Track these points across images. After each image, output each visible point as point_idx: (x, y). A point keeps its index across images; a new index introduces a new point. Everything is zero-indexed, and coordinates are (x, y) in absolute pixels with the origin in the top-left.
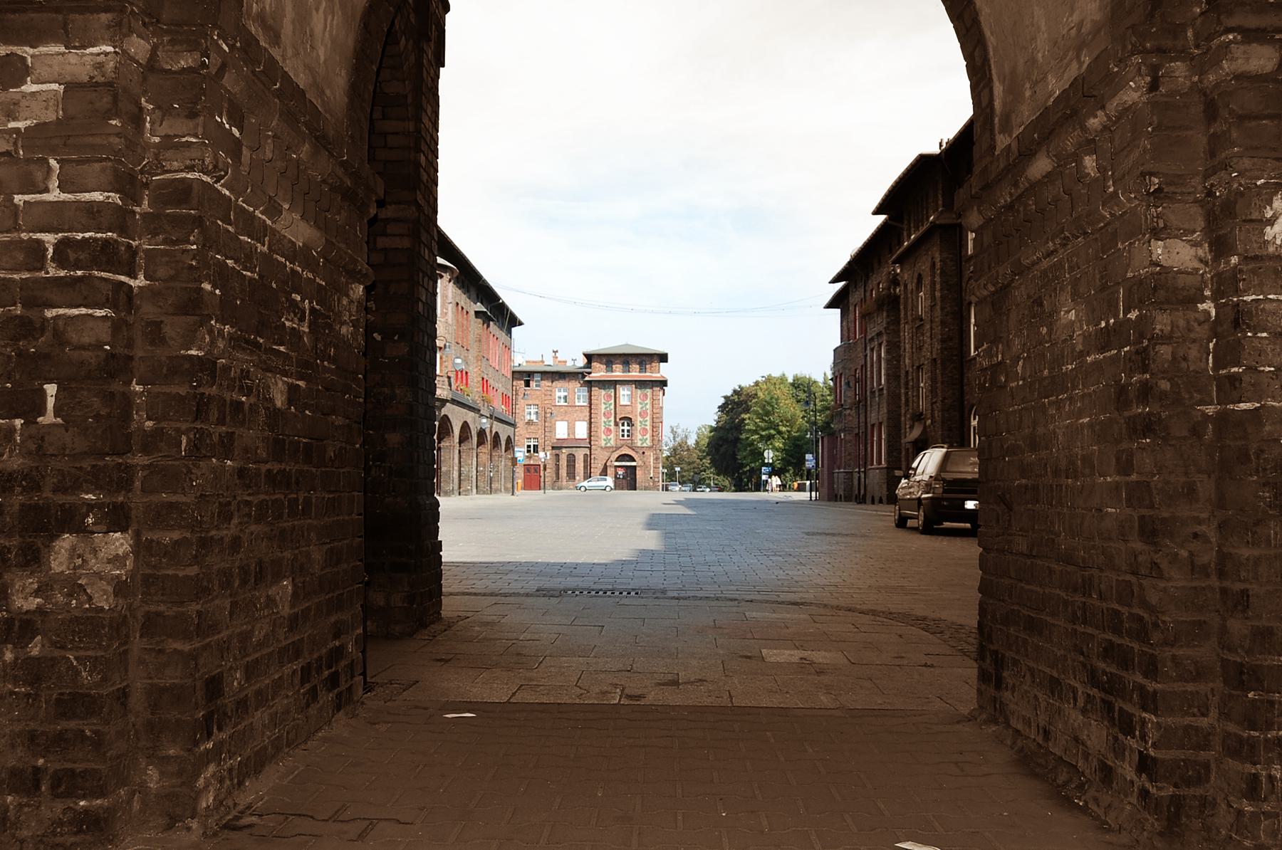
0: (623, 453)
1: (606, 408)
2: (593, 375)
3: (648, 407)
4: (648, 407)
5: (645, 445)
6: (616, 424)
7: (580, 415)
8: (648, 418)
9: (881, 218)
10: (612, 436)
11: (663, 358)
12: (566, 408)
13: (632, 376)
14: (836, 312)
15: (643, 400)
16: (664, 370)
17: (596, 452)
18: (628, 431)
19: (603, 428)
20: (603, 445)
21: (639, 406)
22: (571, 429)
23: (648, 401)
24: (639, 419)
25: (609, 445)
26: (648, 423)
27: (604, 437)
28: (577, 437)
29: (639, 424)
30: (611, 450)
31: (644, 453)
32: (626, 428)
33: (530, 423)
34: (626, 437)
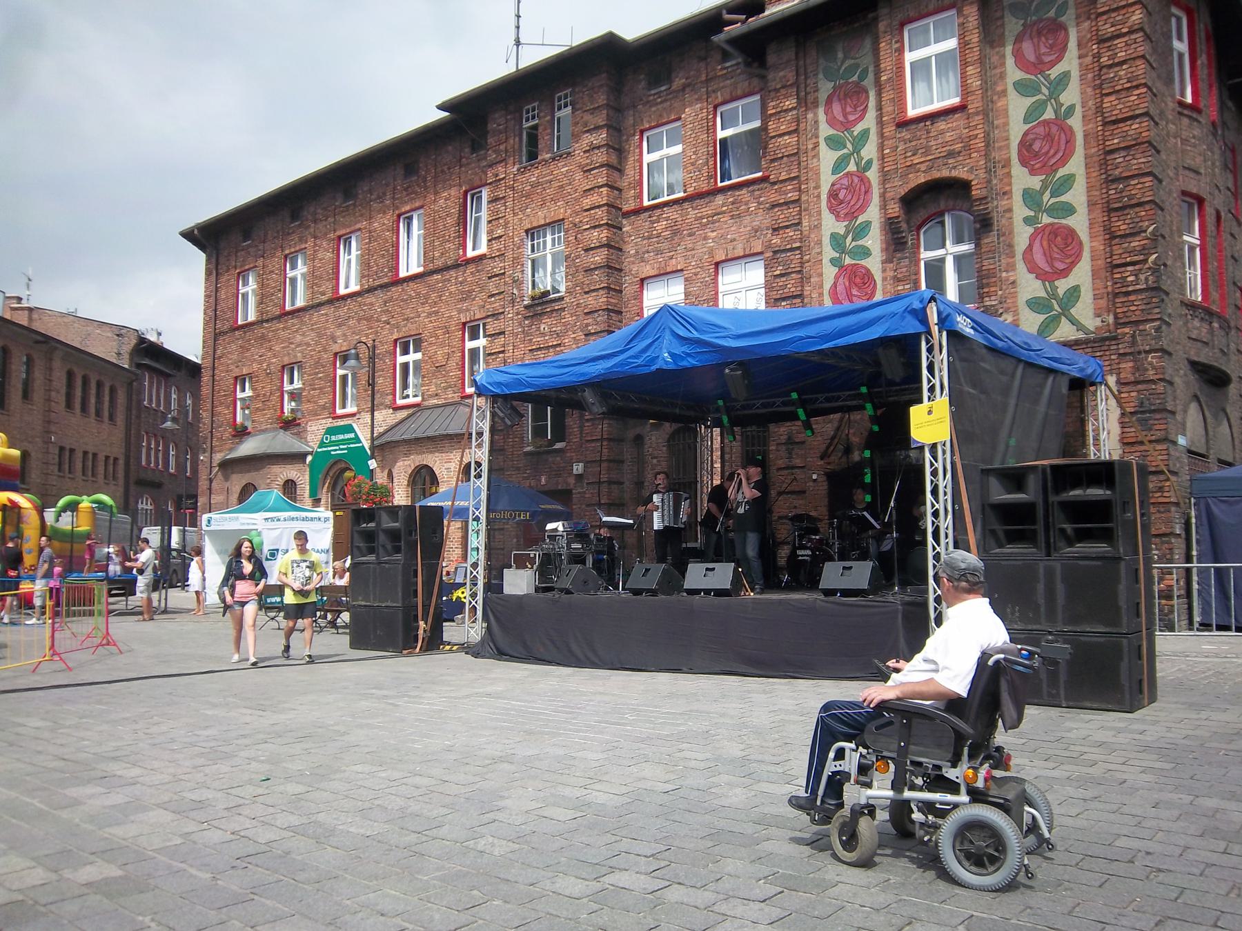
4: (1071, 95)
5: (1066, 331)
8: (1076, 165)
19: (830, 272)
23: (1070, 63)
24: (1022, 179)
26: (1077, 196)
29: (1021, 211)
33: (542, 304)
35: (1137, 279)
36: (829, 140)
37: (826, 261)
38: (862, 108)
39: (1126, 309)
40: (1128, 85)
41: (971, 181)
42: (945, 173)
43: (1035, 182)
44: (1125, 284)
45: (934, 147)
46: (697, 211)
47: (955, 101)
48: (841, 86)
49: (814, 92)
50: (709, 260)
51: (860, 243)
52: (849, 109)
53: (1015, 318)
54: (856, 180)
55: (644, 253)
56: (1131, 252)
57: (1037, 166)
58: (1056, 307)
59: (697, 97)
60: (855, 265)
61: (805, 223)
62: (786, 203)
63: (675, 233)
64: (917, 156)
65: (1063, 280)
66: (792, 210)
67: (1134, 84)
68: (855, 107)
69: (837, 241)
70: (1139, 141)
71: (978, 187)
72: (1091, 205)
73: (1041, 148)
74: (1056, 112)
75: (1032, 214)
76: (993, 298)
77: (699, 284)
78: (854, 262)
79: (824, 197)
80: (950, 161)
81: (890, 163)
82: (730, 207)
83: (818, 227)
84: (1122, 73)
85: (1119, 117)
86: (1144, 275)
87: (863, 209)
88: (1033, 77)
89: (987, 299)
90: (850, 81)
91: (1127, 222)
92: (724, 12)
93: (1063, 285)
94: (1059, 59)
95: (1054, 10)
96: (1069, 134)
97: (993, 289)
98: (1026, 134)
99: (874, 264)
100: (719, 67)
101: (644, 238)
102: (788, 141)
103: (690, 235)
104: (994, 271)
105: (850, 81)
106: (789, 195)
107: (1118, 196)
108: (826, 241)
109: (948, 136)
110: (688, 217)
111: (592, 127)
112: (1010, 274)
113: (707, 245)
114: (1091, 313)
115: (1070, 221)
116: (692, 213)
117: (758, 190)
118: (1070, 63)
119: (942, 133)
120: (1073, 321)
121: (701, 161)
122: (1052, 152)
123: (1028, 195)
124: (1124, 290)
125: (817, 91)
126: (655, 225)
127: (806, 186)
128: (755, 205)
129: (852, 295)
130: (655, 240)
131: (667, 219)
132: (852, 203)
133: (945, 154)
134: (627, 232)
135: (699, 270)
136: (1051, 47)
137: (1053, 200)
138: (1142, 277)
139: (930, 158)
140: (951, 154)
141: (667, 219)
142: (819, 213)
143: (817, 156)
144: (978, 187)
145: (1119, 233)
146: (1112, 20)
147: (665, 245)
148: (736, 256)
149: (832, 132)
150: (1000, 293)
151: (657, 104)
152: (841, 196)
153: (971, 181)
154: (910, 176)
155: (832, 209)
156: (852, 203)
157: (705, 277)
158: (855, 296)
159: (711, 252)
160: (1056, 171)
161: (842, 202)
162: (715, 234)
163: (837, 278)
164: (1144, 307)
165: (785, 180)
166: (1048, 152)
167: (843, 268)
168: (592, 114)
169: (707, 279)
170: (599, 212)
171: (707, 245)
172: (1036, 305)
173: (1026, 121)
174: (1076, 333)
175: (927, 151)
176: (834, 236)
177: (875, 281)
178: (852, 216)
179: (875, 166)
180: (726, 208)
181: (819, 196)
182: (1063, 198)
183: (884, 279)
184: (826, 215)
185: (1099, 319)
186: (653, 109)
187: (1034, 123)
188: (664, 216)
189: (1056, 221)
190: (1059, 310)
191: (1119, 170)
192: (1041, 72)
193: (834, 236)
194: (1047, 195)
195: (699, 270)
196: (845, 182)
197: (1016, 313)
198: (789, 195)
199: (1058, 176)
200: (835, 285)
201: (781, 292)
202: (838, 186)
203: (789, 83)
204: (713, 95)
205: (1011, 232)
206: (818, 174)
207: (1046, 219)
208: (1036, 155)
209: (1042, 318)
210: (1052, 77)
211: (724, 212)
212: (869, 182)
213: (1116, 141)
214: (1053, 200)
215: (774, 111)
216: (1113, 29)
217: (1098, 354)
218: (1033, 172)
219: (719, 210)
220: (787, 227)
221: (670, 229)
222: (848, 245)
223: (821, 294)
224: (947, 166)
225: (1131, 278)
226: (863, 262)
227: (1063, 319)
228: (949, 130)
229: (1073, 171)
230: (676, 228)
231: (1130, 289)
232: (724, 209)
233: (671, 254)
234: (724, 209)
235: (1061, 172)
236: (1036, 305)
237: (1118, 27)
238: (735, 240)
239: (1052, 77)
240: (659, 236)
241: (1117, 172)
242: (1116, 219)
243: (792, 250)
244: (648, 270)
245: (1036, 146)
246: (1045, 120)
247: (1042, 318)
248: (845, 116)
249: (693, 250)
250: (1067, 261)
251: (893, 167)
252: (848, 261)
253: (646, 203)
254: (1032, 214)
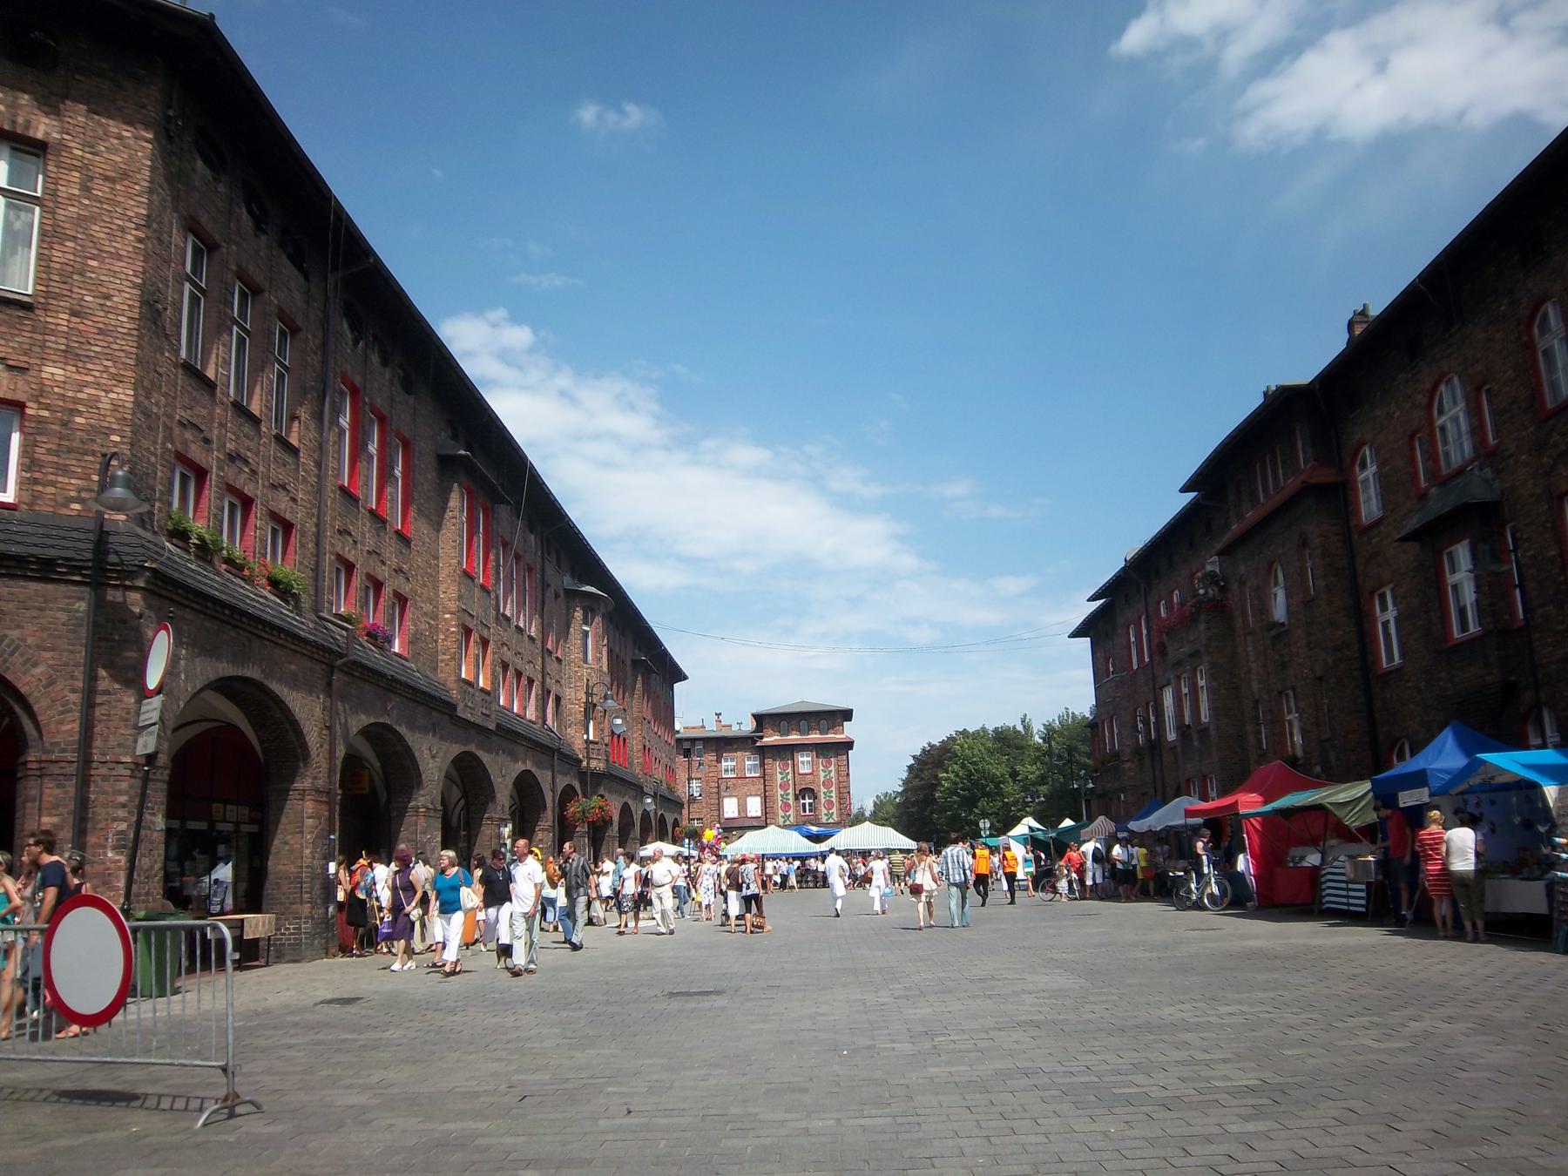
2: (765, 740)
3: (832, 774)
4: (832, 774)
5: (831, 821)
6: (796, 798)
8: (833, 788)
9: (1191, 495)
10: (791, 812)
11: (847, 715)
14: (1085, 642)
15: (826, 767)
16: (849, 730)
18: (810, 804)
19: (780, 803)
21: (822, 774)
22: (742, 807)
23: (832, 768)
24: (823, 790)
26: (833, 794)
27: (781, 813)
28: (749, 815)
29: (823, 796)
32: (807, 801)
34: (807, 813)
47: (810, 771)
99: (791, 802)
118: (832, 768)
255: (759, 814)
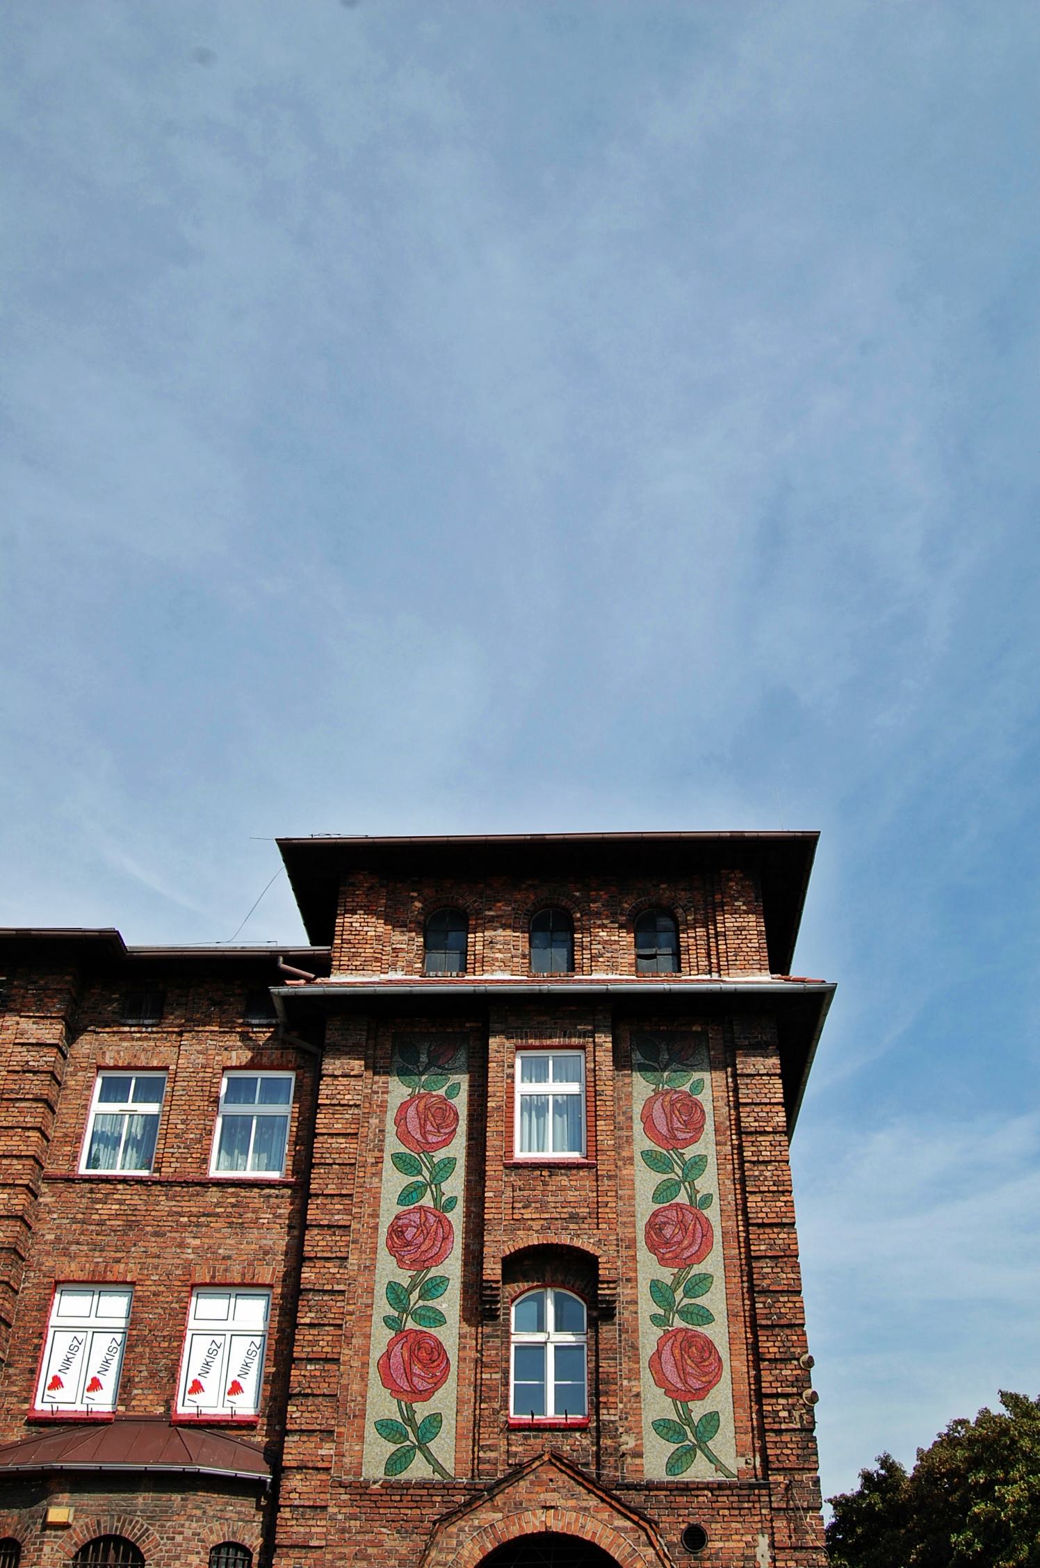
0: (534, 1522)
1: (404, 1198)
4: (708, 1182)
5: (700, 1471)
7: (228, 1244)
8: (714, 1264)
12: (135, 1198)
13: (598, 982)
17: (317, 1530)
19: (381, 1337)
20: (374, 1471)
21: (646, 1181)
23: (706, 1146)
24: (649, 1268)
25: (419, 1469)
26: (716, 1300)
28: (185, 1407)
29: (647, 1307)
30: (432, 1513)
31: (695, 1538)
35: (790, 1416)
36: (397, 1158)
37: (377, 1319)
38: (447, 1131)
39: (779, 1452)
40: (775, 1188)
41: (600, 1257)
42: (565, 1240)
43: (667, 1275)
44: (777, 1419)
45: (553, 1205)
46: (174, 1203)
48: (421, 1097)
49: (383, 1093)
50: (182, 1278)
51: (430, 1303)
52: (429, 1127)
53: (639, 1442)
54: (432, 1219)
55: (70, 1243)
56: (783, 1381)
57: (667, 1256)
58: (690, 1435)
59: (199, 1048)
60: (422, 1332)
61: (353, 1259)
62: (329, 1226)
63: (130, 1225)
64: (529, 1210)
65: (699, 1403)
66: (338, 1238)
67: (780, 1189)
68: (439, 1127)
69: (396, 1294)
70: (788, 1253)
71: (606, 1266)
72: (731, 1315)
73: (673, 1236)
74: (690, 1197)
75: (661, 1312)
76: (612, 1411)
77: (160, 1311)
78: (419, 1328)
79: (383, 1231)
80: (571, 1226)
81: (493, 1211)
82: (229, 1210)
83: (370, 1269)
84: (768, 1174)
85: (766, 1221)
86: (798, 1413)
87: (438, 1259)
88: (665, 1152)
89: (605, 1411)
90: (434, 1093)
91: (777, 1344)
92: (281, 959)
93: (698, 1409)
94: (694, 1140)
95: (689, 1085)
96: (707, 1225)
97: (611, 1399)
98: (655, 1215)
100: (241, 1021)
101: (74, 1220)
102: (343, 1146)
103: (156, 1234)
104: (615, 1376)
105: (434, 1093)
106: (337, 1217)
107: (767, 1311)
108: (380, 1290)
109: (571, 1196)
110: (157, 1208)
111: (35, 1041)
112: (633, 1383)
113: (183, 1256)
114: (733, 1452)
115: (706, 1330)
116: (165, 1205)
117: (277, 1197)
119: (563, 1189)
120: (711, 1458)
121: (192, 1136)
122: (686, 1242)
123: (656, 1287)
124: (776, 1426)
125: (387, 1093)
126: (98, 1206)
127: (359, 1210)
128: (271, 1216)
129: (412, 1374)
130: (93, 1227)
131: (121, 1202)
132: (423, 1248)
133: (567, 1216)
134: (46, 1205)
135: (162, 1288)
136: (686, 1123)
137: (686, 1301)
138: (796, 1414)
139: (546, 1216)
140: (573, 1217)
141: (121, 1202)
142: (374, 1250)
143: (378, 1174)
144: (606, 1266)
145: (769, 1356)
146: (755, 1115)
147: (112, 1239)
148: (228, 1281)
149: (403, 1149)
150: (621, 1406)
151: (133, 1039)
152: (409, 1235)
153: (600, 1257)
154: (518, 1232)
155: (392, 1250)
156: (423, 1248)
157: (172, 1302)
158: (415, 1374)
159: (188, 1267)
160: (690, 1266)
161: (408, 1244)
162: (198, 1242)
163: (391, 1344)
164: (799, 1452)
165: (332, 1196)
166: (680, 1243)
167: (401, 1333)
168: (34, 1023)
169: (174, 1305)
170: (17, 1165)
171: (183, 1256)
172: (665, 1428)
173: (655, 1199)
174: (714, 1474)
175: (543, 1206)
176: (392, 1287)
177: (448, 1359)
178: (422, 1264)
179: (460, 1208)
180: (222, 1210)
181: (376, 1228)
182: (698, 1301)
183: (461, 1360)
184: (383, 1253)
185: (743, 1460)
186: (125, 1044)
187: (665, 1205)
188: (115, 1196)
189: (690, 1327)
190: (693, 1440)
191: (768, 1282)
192: (675, 1149)
193: (392, 1287)
194: (679, 1294)
195: (162, 1288)
196: (416, 1217)
197: (639, 1436)
198: (337, 1217)
199: (692, 1273)
200: (388, 1354)
201: (310, 1349)
202: (406, 1221)
203: (352, 1073)
204: (225, 1053)
205: (635, 1331)
206: (377, 1198)
207: (678, 1323)
208: (667, 1243)
209: (674, 1447)
210: (687, 1157)
211: (218, 1215)
212: (451, 1226)
213: (763, 1247)
214: (686, 1301)
215: (328, 1102)
216: (757, 1124)
217: (746, 1505)
218: (663, 1261)
219: (209, 1210)
220: (327, 1259)
221: (124, 1218)
222: (412, 1303)
223: (365, 1364)
224: (568, 1232)
225: (784, 1414)
226: (432, 1331)
227: (699, 1452)
228: (576, 1189)
229: (710, 1271)
230: (134, 1218)
231: (783, 1426)
232: (218, 1210)
233: (119, 1255)
234: (218, 1210)
235: (696, 1269)
236: (665, 1428)
237: (761, 1124)
238: (229, 1258)
239: (687, 1157)
240: (101, 1223)
241: (765, 1283)
242: (765, 1338)
243: (332, 1292)
244: (72, 1269)
245: (668, 1232)
246: (678, 1204)
247: (674, 1447)
248: (424, 1135)
249: (158, 1257)
250: (704, 1379)
251: (496, 1216)
252: (410, 1324)
253: (83, 1170)
254: (661, 1312)
255: (246, 1405)
